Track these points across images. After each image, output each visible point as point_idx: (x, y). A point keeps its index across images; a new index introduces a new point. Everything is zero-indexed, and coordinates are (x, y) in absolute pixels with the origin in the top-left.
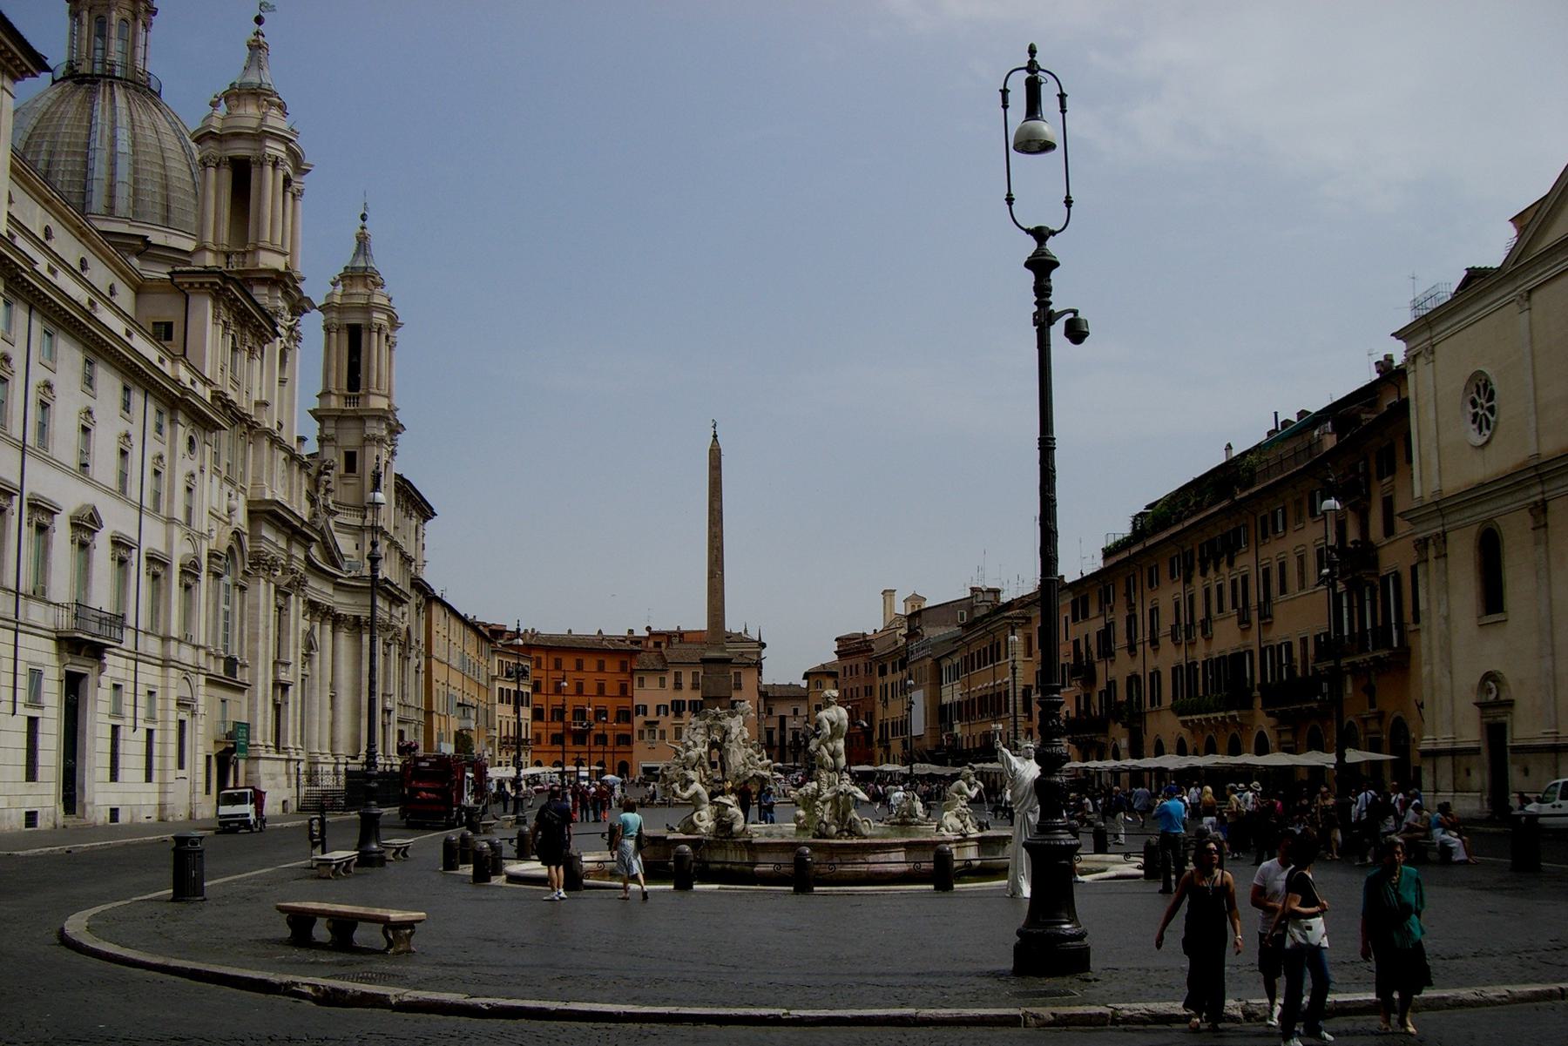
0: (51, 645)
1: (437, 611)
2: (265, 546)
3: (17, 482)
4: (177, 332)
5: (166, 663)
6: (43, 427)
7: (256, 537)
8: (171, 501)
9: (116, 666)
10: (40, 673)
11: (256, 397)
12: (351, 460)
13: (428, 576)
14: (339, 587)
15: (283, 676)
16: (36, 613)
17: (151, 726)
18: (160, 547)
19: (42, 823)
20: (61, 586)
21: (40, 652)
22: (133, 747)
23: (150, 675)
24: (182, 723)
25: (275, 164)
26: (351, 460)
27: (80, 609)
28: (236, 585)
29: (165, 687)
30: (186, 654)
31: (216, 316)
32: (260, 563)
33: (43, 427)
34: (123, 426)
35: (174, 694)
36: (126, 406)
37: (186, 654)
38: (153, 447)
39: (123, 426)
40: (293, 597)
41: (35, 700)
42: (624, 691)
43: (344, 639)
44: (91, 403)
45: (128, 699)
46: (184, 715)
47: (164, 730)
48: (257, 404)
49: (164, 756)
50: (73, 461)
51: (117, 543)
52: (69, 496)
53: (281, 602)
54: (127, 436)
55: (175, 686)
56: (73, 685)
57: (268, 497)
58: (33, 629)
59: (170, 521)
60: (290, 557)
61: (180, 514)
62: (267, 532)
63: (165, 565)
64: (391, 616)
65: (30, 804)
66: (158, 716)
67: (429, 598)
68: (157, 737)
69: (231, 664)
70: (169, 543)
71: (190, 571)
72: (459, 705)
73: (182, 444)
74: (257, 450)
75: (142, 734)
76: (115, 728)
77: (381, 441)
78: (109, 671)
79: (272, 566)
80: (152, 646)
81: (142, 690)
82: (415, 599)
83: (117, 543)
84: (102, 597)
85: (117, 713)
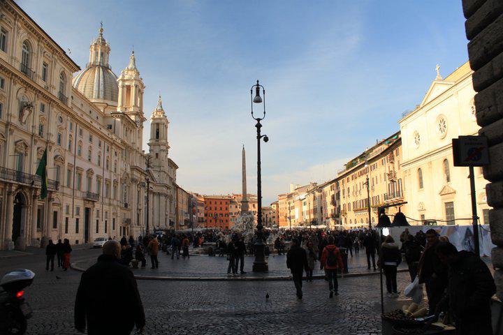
4: (113, 127)
5: (110, 205)
6: (80, 151)
9: (98, 206)
11: (132, 141)
12: (157, 154)
13: (178, 183)
15: (139, 208)
16: (78, 194)
18: (108, 177)
19: (79, 243)
20: (84, 187)
21: (80, 203)
22: (102, 225)
23: (106, 208)
24: (114, 219)
25: (136, 86)
26: (157, 154)
27: (89, 194)
30: (115, 203)
31: (122, 123)
32: (133, 180)
33: (80, 151)
35: (112, 212)
36: (100, 145)
37: (115, 203)
38: (106, 154)
41: (78, 214)
42: (226, 209)
43: (155, 197)
45: (101, 213)
46: (114, 217)
47: (110, 221)
48: (133, 143)
49: (109, 227)
50: (87, 158)
51: (98, 176)
52: (86, 166)
54: (100, 152)
55: (111, 210)
56: (87, 211)
58: (77, 198)
59: (111, 171)
61: (113, 170)
62: (135, 173)
65: (77, 238)
67: (177, 187)
69: (126, 205)
70: (110, 177)
71: (115, 182)
73: (114, 153)
75: (104, 221)
76: (97, 221)
77: (164, 151)
79: (136, 181)
80: (107, 201)
81: (104, 212)
82: (173, 187)
83: (98, 176)
84: (94, 190)
85: (98, 216)
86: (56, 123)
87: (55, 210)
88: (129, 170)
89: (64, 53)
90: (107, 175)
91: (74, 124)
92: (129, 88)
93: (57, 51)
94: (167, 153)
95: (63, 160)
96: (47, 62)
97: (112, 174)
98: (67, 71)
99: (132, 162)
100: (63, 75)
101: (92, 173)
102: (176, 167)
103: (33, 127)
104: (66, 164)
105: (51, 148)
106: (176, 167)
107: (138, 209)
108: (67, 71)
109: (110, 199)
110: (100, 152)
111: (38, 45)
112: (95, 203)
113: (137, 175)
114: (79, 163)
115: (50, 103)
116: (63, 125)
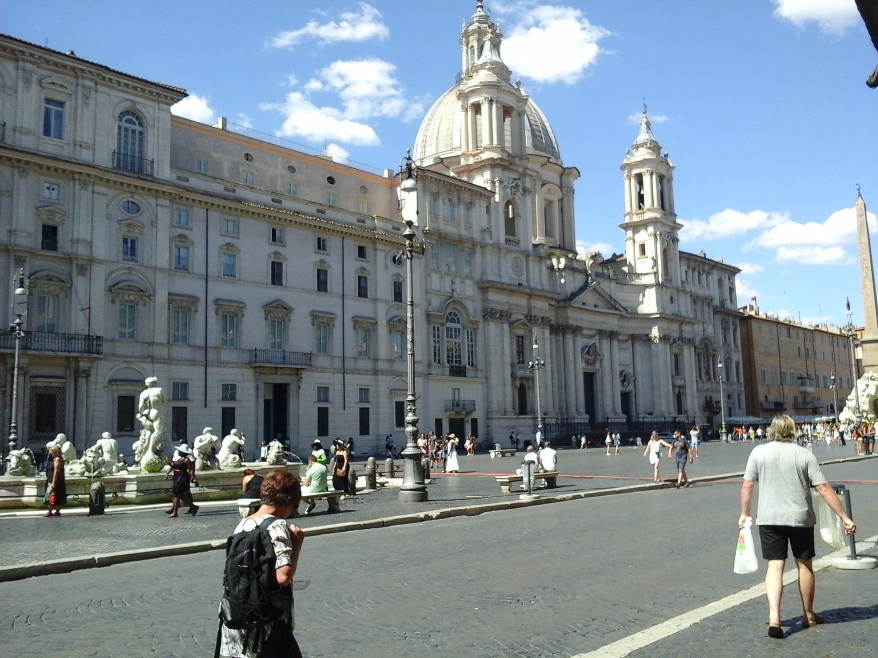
0: (249, 372)
1: (755, 325)
2: (491, 305)
3: (201, 295)
5: (376, 373)
7: (485, 300)
8: (376, 291)
10: (234, 387)
14: (622, 317)
16: (227, 355)
17: (364, 405)
25: (491, 102)
28: (464, 328)
29: (377, 386)
34: (318, 257)
39: (318, 257)
40: (535, 330)
44: (281, 250)
48: (483, 231)
53: (520, 332)
57: (492, 277)
59: (375, 300)
60: (530, 308)
62: (493, 296)
63: (376, 323)
64: (681, 331)
66: (371, 399)
67: (746, 320)
68: (371, 412)
70: (376, 312)
72: (799, 378)
74: (483, 255)
78: (304, 380)
79: (503, 316)
83: (315, 316)
86: (109, 216)
87: (125, 393)
88: (468, 289)
89: (107, 69)
90: (357, 307)
91: (199, 213)
92: (477, 108)
93: (83, 71)
94: (676, 240)
95: (145, 294)
96: (60, 98)
97: (382, 309)
98: (147, 107)
99: (483, 273)
100: (131, 115)
101: (287, 310)
102: (734, 271)
103: (10, 232)
104: (162, 297)
105: (82, 270)
106: (734, 271)
107: (513, 376)
108: (147, 107)
109: (376, 360)
110: (322, 261)
111: (17, 68)
112: (305, 374)
113: (497, 299)
114: (220, 290)
115: (74, 179)
116: (145, 218)
